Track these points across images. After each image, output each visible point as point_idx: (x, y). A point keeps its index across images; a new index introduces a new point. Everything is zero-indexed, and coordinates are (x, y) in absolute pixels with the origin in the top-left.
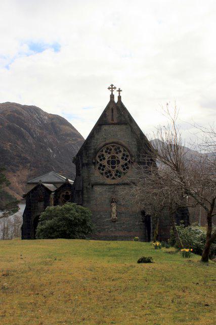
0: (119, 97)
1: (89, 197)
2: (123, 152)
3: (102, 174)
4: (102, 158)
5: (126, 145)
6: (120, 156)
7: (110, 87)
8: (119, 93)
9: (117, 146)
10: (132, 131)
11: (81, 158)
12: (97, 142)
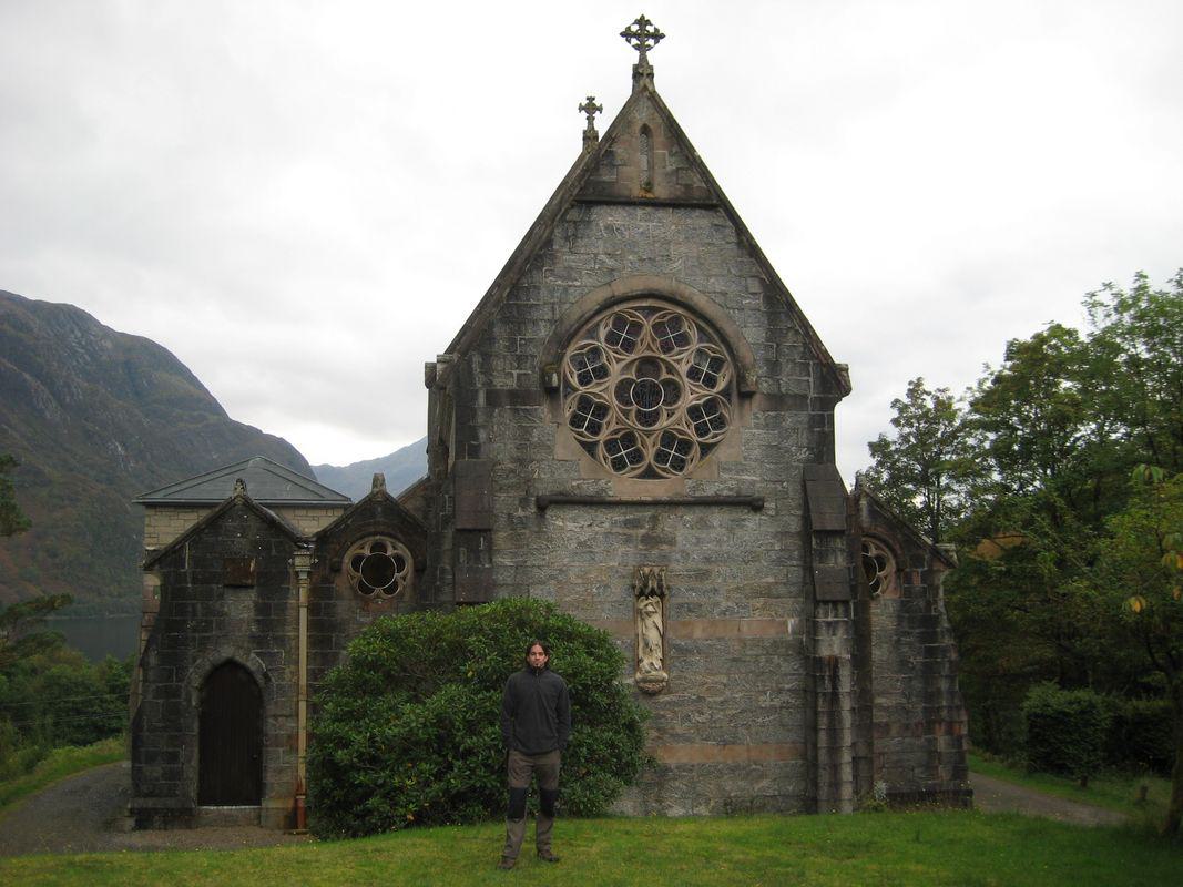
1: (519, 567)
2: (695, 345)
3: (590, 448)
5: (712, 310)
6: (683, 361)
7: (635, 28)
8: (590, 119)
9: (671, 312)
10: (740, 244)
11: (487, 370)
12: (566, 289)
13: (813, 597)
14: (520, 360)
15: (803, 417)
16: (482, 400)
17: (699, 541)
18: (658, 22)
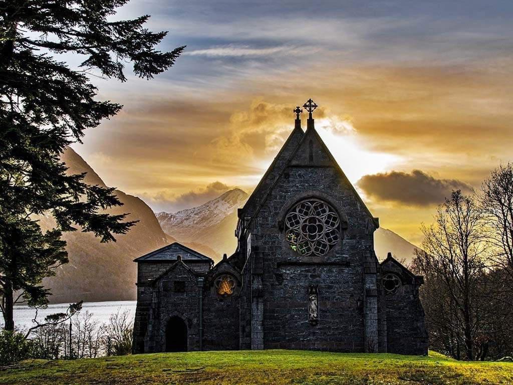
0: (311, 122)
2: (327, 213)
6: (323, 218)
17: (329, 276)
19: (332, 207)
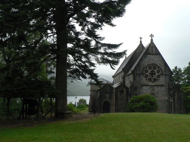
2: (157, 69)
4: (147, 71)
6: (156, 71)
9: (155, 66)
13: (170, 95)
14: (140, 70)
15: (168, 77)
16: (136, 75)
18: (153, 35)
19: (159, 67)
